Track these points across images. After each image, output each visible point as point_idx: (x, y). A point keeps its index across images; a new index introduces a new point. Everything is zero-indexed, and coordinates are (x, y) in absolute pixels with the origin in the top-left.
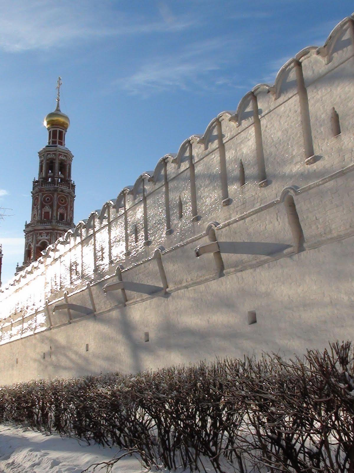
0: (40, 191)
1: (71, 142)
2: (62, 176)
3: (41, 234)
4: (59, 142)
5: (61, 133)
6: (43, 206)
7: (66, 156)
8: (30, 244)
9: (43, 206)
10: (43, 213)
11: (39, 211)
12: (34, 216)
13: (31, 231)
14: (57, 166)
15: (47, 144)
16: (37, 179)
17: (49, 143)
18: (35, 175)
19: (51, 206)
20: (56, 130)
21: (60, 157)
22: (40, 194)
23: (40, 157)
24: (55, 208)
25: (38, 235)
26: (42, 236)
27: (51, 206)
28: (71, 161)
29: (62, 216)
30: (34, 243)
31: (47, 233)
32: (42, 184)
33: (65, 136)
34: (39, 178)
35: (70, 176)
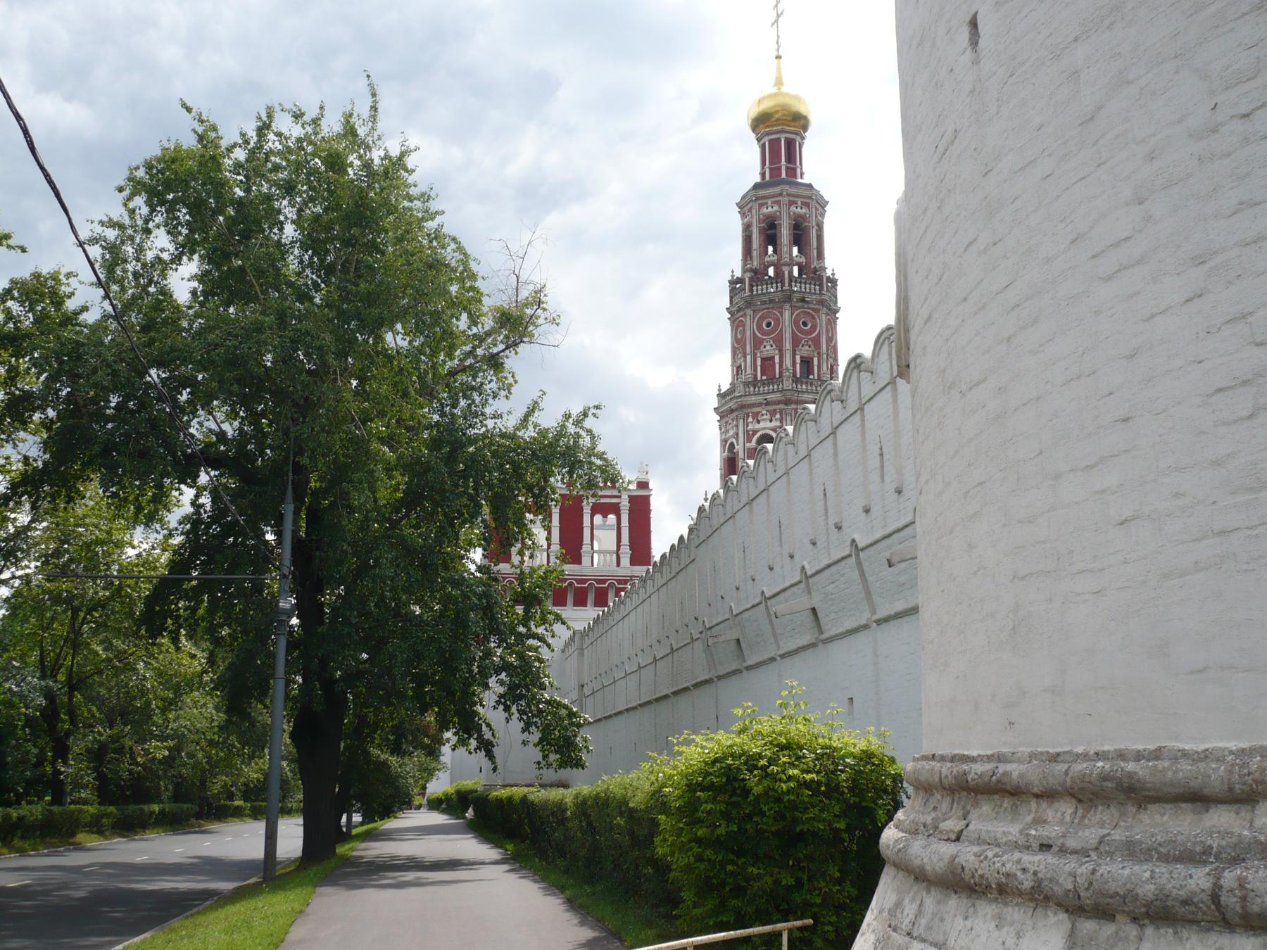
0: (749, 304)
1: (817, 165)
2: (803, 260)
3: (756, 415)
4: (787, 168)
5: (790, 144)
6: (757, 344)
7: (807, 205)
8: (732, 444)
9: (757, 344)
10: (759, 363)
11: (748, 357)
12: (738, 370)
13: (732, 411)
14: (785, 233)
15: (758, 179)
16: (738, 274)
17: (763, 175)
18: (732, 262)
19: (779, 342)
20: (779, 139)
21: (793, 208)
22: (749, 312)
23: (743, 215)
24: (788, 345)
25: (750, 419)
26: (759, 422)
27: (779, 342)
28: (823, 215)
29: (807, 363)
30: (741, 440)
31: (773, 413)
32: (751, 286)
33: (804, 150)
34: (744, 271)
35: (820, 256)
